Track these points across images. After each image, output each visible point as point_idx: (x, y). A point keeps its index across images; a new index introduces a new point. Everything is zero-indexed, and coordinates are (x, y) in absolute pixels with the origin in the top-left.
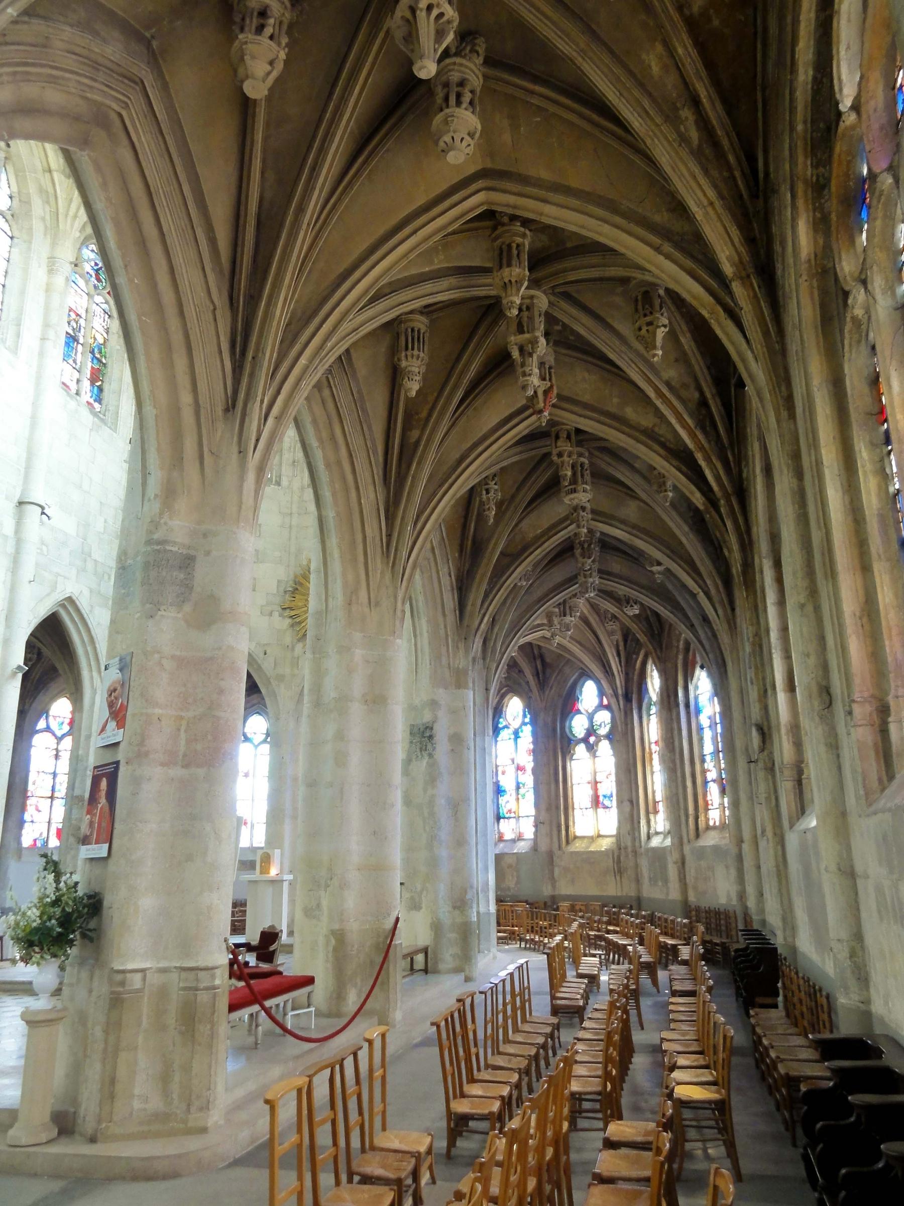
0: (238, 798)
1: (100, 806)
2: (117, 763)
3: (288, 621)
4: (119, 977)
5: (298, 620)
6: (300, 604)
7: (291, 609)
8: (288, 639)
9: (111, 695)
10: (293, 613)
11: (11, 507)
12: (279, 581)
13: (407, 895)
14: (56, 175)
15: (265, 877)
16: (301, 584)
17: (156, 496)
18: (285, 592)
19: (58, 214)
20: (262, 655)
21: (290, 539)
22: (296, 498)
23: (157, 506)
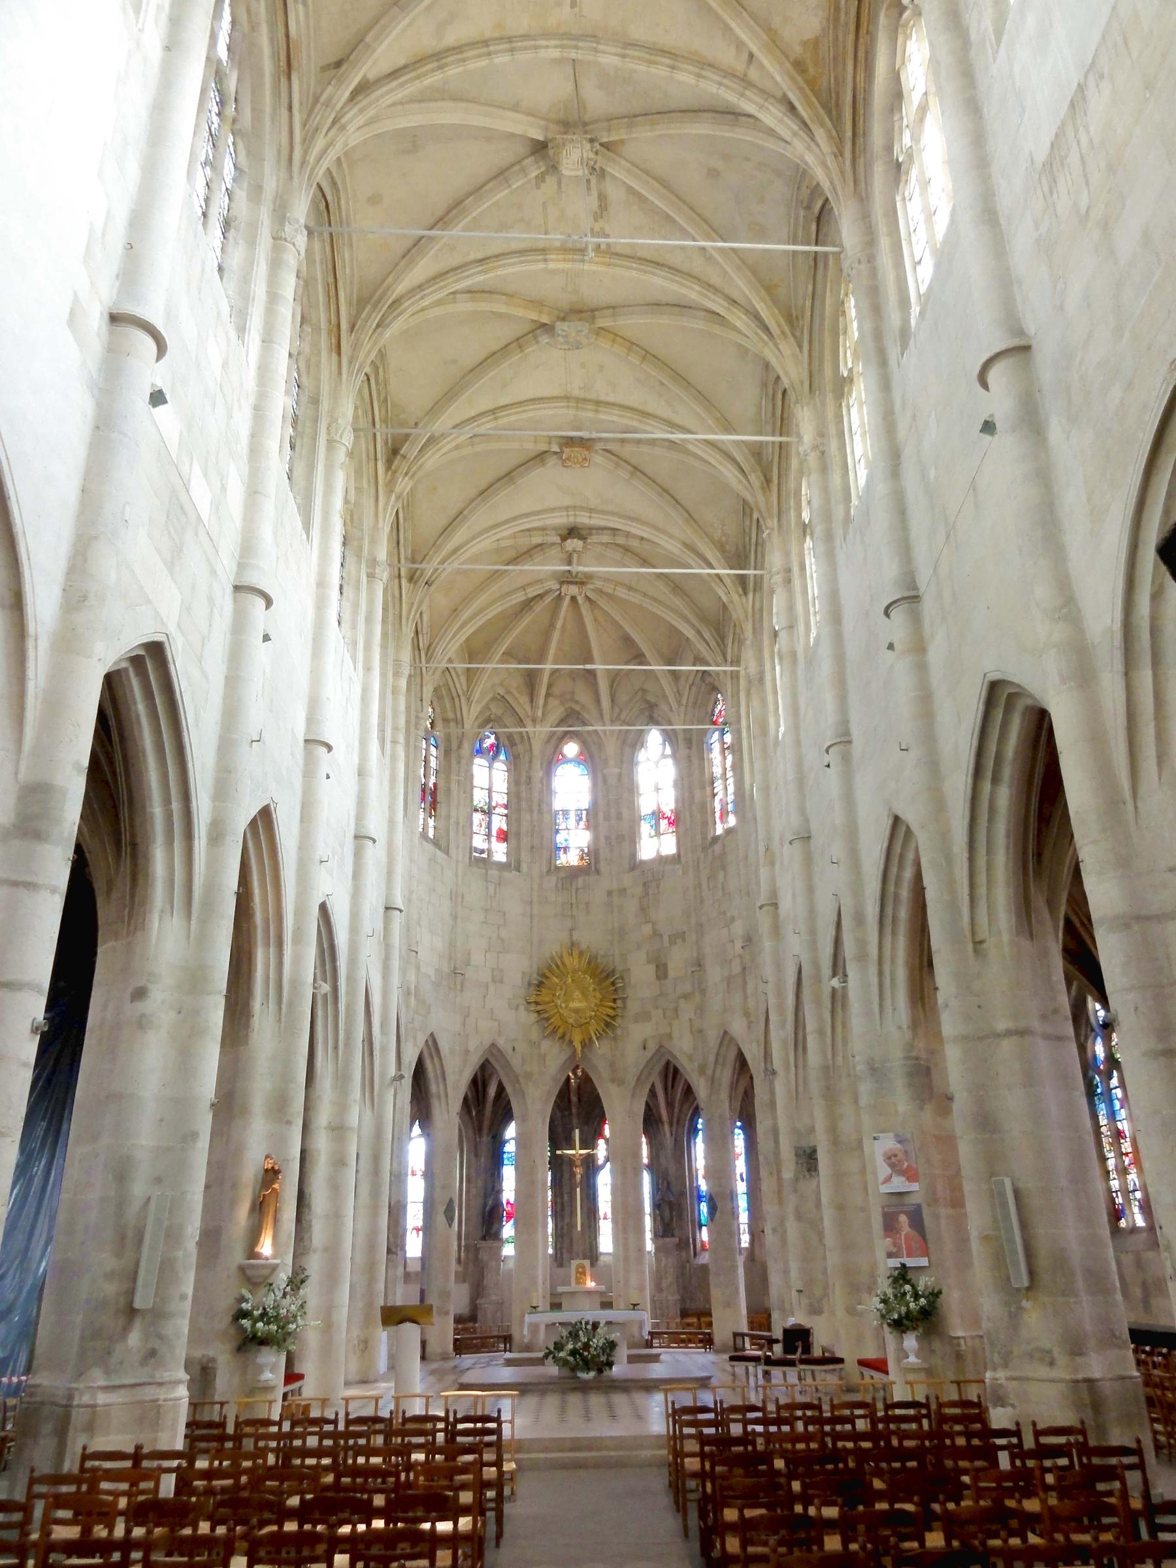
0: (409, 1200)
1: (903, 1234)
2: (919, 1206)
3: (533, 1017)
4: (955, 1341)
5: (546, 1015)
6: (547, 999)
7: (537, 1003)
8: (535, 1034)
9: (890, 1158)
10: (539, 1008)
11: (382, 910)
12: (523, 973)
13: (805, 1301)
14: (404, 582)
15: (580, 1288)
16: (547, 978)
17: (908, 1028)
18: (530, 984)
19: (401, 617)
20: (510, 1051)
21: (531, 928)
22: (535, 887)
23: (908, 1034)
